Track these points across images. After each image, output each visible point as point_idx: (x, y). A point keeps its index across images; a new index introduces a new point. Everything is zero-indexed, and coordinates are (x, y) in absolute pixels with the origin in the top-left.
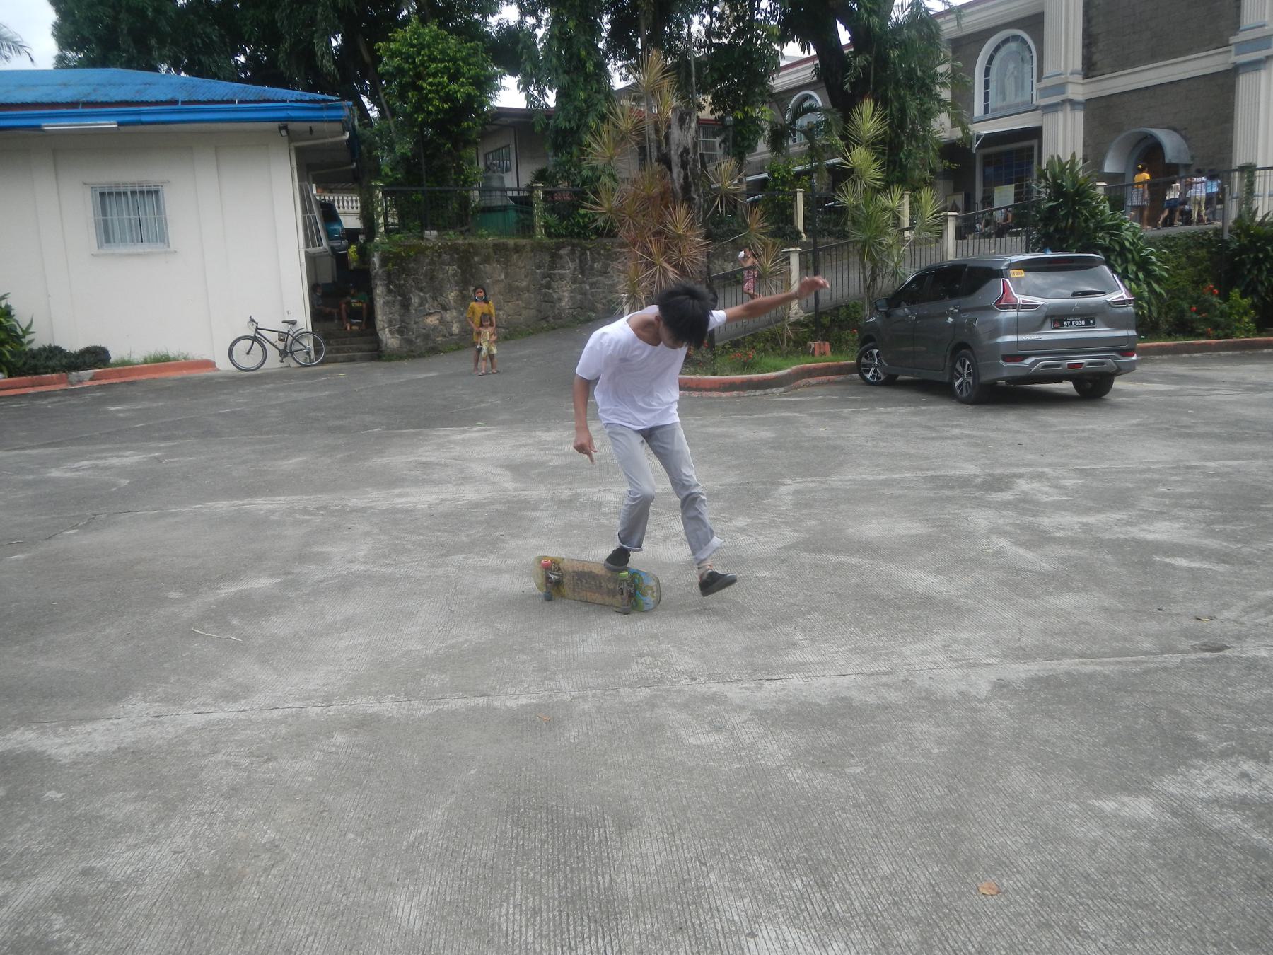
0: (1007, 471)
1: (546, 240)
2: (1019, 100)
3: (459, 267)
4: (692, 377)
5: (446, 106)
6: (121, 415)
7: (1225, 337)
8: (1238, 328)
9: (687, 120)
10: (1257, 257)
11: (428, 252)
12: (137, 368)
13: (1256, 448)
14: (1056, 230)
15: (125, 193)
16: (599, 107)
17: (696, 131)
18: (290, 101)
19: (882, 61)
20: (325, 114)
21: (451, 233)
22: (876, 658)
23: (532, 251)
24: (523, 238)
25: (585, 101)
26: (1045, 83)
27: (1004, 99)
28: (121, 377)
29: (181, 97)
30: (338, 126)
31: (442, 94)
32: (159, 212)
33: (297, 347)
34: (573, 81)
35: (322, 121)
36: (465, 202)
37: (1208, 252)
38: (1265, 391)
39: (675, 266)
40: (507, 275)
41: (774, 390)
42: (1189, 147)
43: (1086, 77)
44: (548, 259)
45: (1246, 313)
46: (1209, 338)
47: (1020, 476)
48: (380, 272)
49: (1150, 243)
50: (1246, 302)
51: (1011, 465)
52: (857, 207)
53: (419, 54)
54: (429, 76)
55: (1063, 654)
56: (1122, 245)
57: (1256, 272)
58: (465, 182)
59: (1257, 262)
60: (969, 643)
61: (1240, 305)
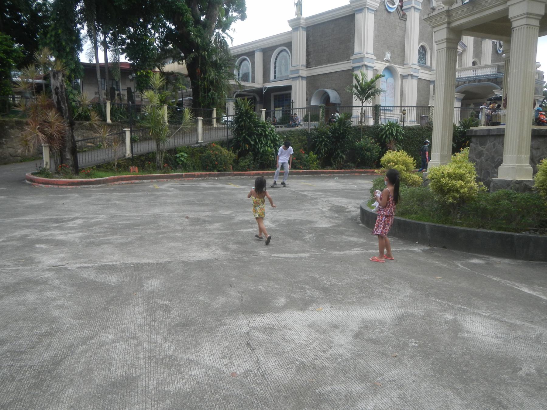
2: (286, 75)
4: (55, 179)
7: (307, 169)
9: (57, 75)
10: (320, 140)
17: (62, 80)
27: (281, 74)
41: (95, 186)
43: (307, 68)
45: (317, 161)
46: (301, 169)
50: (315, 156)
56: (265, 133)
57: (320, 145)
59: (321, 142)
61: (312, 158)
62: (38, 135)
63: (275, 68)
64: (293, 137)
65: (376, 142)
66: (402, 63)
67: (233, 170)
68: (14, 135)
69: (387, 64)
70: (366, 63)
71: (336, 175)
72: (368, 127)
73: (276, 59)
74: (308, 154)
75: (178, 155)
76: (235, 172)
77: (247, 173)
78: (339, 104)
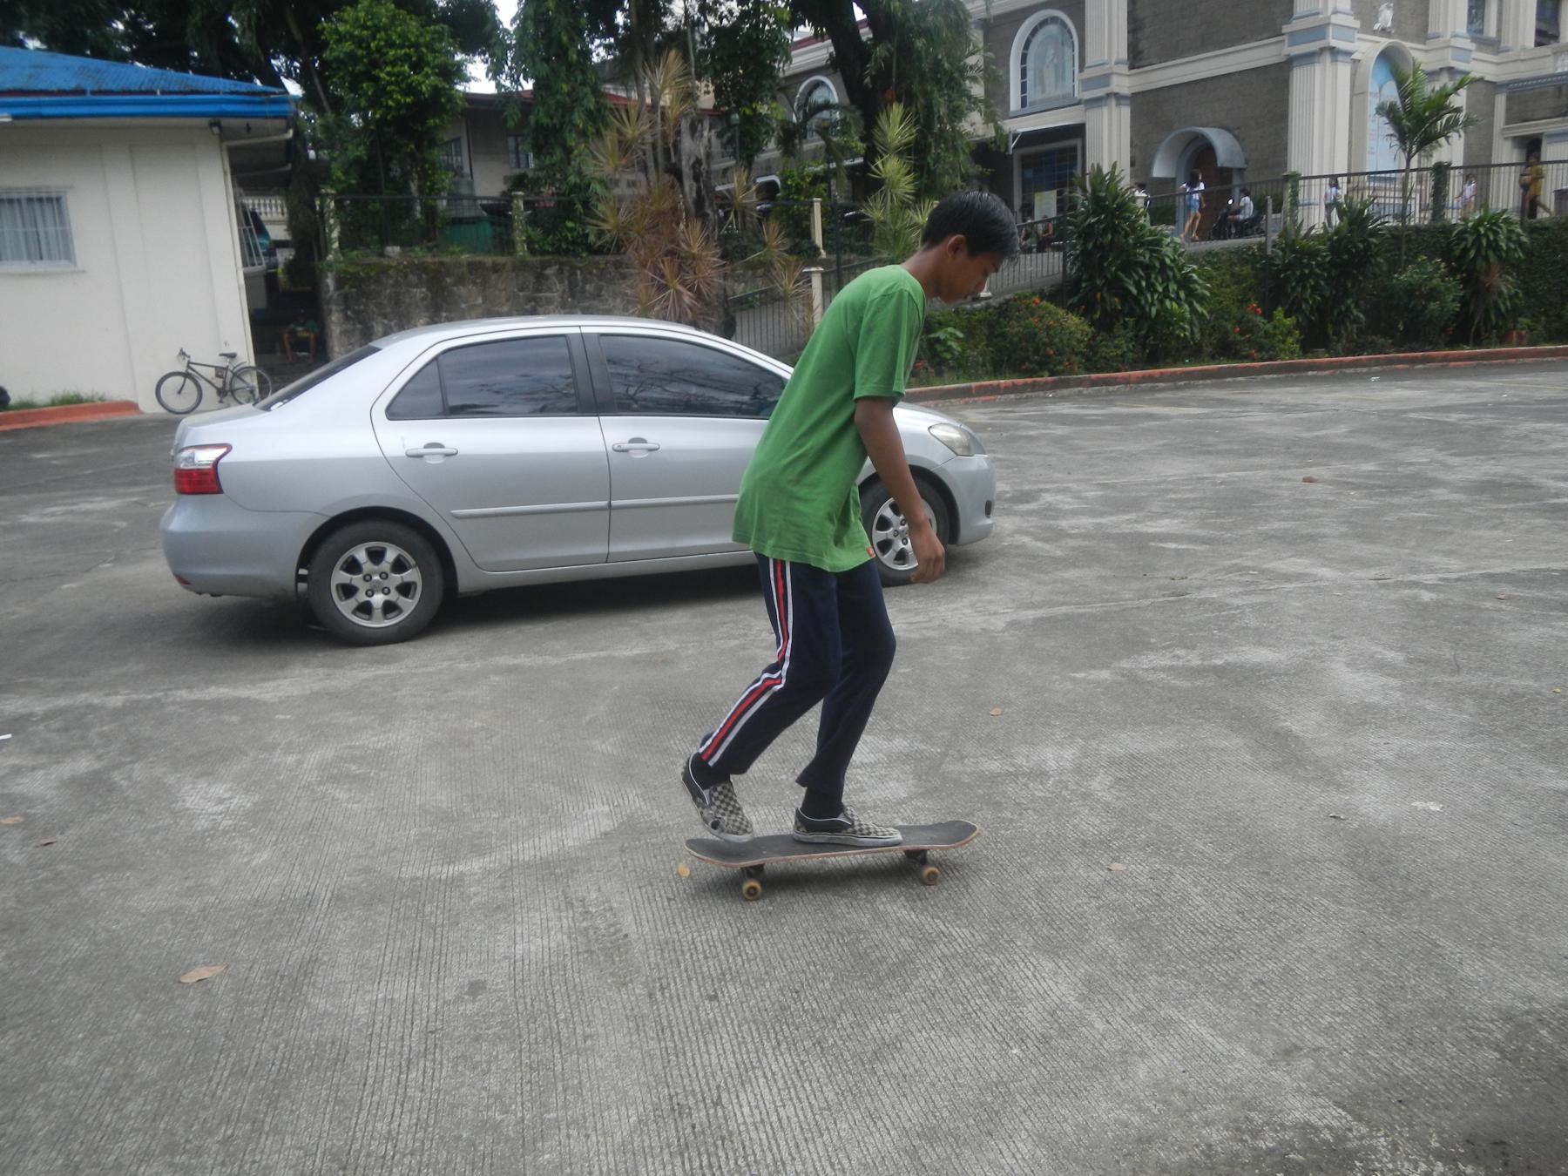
0: (1035, 487)
1: (529, 258)
2: (1059, 92)
3: (428, 289)
5: (408, 100)
6: (55, 462)
7: (1270, 359)
8: (1282, 350)
10: (1303, 274)
11: (392, 272)
12: (44, 413)
13: (1267, 461)
14: (1095, 246)
15: (19, 201)
16: (585, 101)
18: (225, 93)
19: (905, 51)
20: (268, 108)
21: (417, 249)
22: (916, 614)
23: (513, 270)
24: (502, 255)
25: (569, 94)
26: (1088, 73)
27: (1043, 91)
28: (24, 422)
29: (89, 85)
30: (281, 123)
31: (404, 86)
32: (63, 223)
33: (238, 384)
34: (553, 70)
35: (266, 117)
36: (430, 212)
37: (1253, 268)
38: (1295, 411)
39: (690, 290)
40: (485, 299)
42: (1243, 149)
43: (1132, 67)
44: (532, 280)
45: (1290, 333)
46: (1254, 360)
47: (1047, 491)
48: (336, 295)
49: (1193, 259)
50: (1289, 322)
51: (1039, 482)
52: (884, 223)
53: (374, 38)
54: (386, 64)
55: (1063, 604)
56: (1163, 263)
58: (431, 189)
59: (1302, 280)
60: (991, 602)
62: (679, 293)
63: (1024, 73)
64: (1217, 269)
65: (1452, 272)
66: (1423, 35)
67: (1088, 370)
68: (467, 302)
69: (1385, 42)
70: (1334, 43)
71: (1347, 371)
72: (1417, 229)
73: (1027, 46)
74: (1269, 317)
75: (941, 335)
76: (1094, 376)
77: (1123, 378)
78: (1240, 170)
